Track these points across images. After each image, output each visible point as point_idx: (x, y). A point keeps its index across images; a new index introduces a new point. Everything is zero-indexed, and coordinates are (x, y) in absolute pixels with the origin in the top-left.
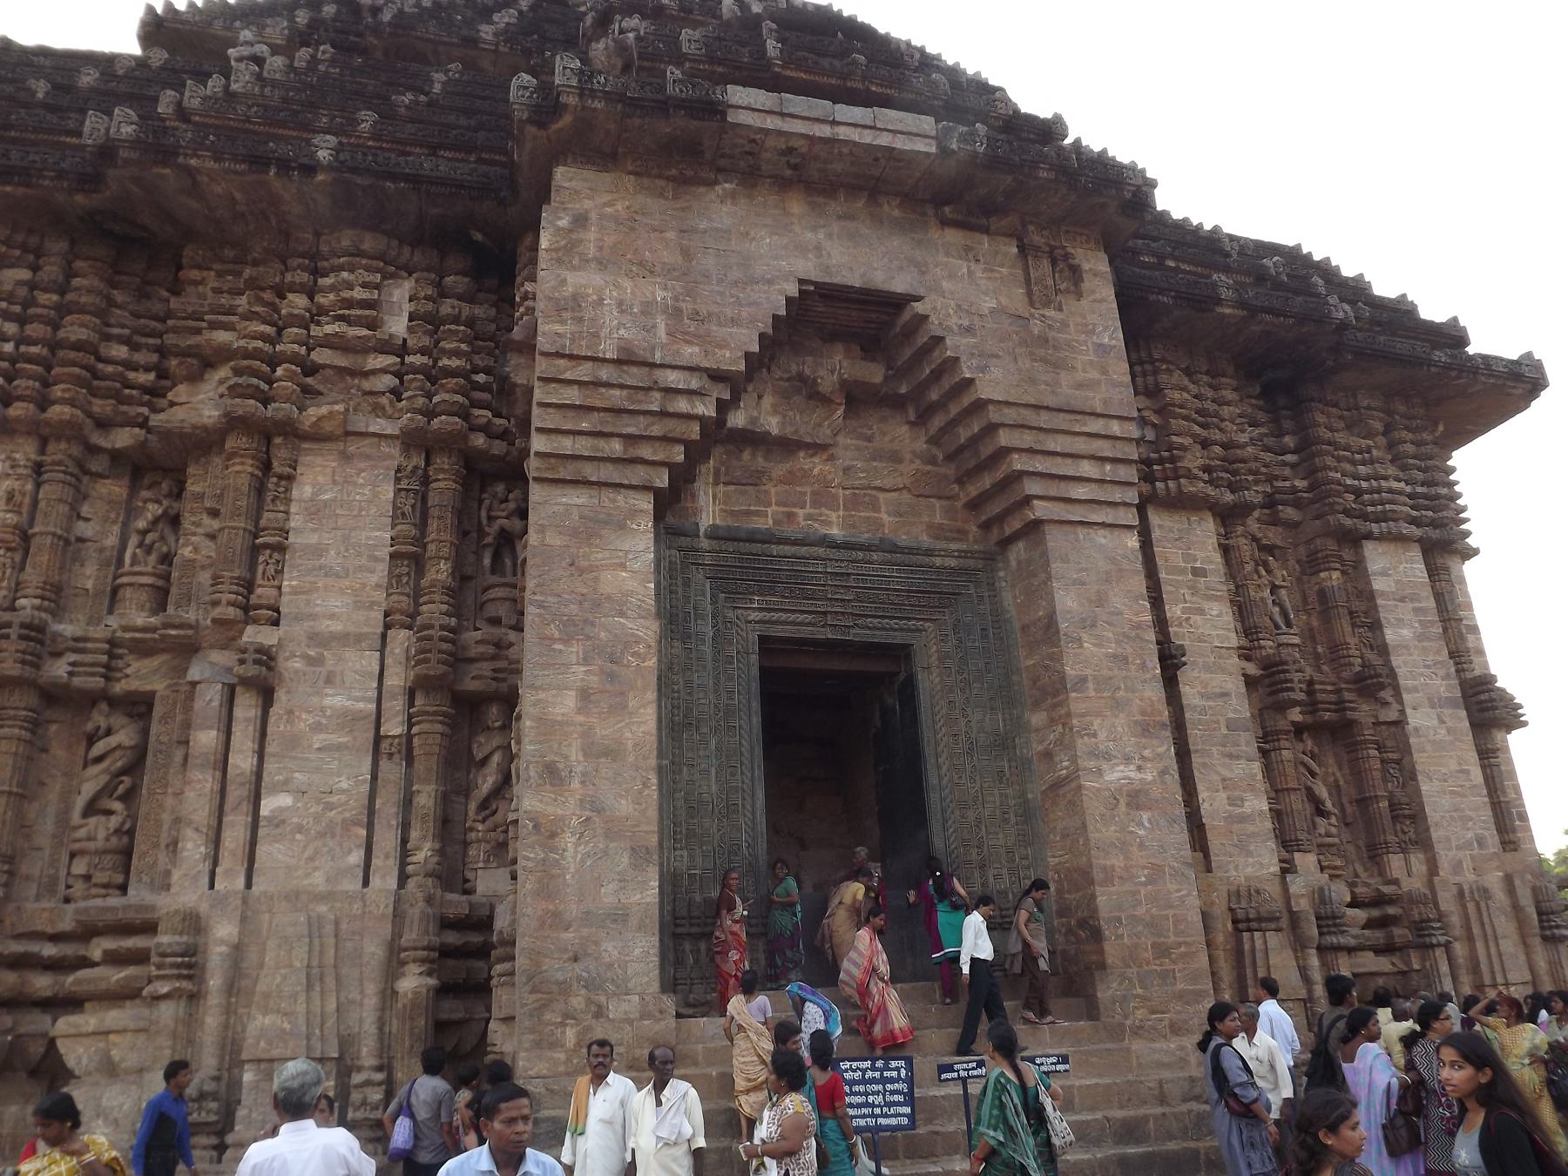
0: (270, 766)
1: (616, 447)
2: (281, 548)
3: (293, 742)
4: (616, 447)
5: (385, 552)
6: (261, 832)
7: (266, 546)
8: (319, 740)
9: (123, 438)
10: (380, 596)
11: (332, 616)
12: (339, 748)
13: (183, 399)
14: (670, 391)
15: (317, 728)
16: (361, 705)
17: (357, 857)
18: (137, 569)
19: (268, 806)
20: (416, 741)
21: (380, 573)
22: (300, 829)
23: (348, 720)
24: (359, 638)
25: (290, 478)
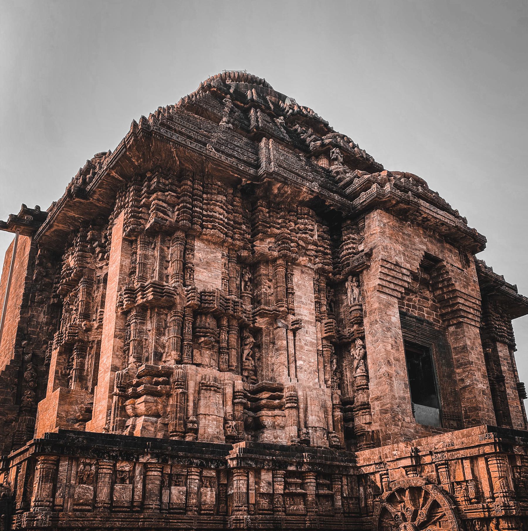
0: (298, 353)
1: (392, 286)
2: (293, 294)
3: (301, 347)
4: (392, 286)
5: (314, 300)
6: (298, 370)
7: (291, 293)
8: (306, 348)
9: (244, 253)
10: (314, 312)
11: (305, 315)
12: (311, 351)
13: (258, 245)
14: (403, 274)
15: (305, 344)
16: (313, 341)
17: (317, 380)
18: (247, 292)
19: (299, 363)
20: (325, 352)
21: (313, 307)
22: (305, 371)
23: (312, 344)
24: (311, 323)
25: (292, 275)
